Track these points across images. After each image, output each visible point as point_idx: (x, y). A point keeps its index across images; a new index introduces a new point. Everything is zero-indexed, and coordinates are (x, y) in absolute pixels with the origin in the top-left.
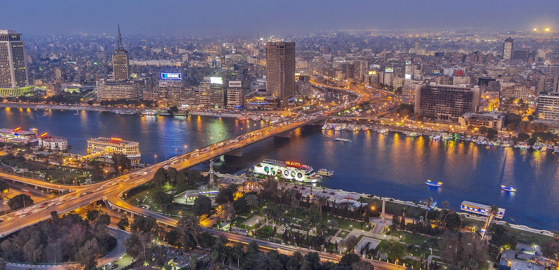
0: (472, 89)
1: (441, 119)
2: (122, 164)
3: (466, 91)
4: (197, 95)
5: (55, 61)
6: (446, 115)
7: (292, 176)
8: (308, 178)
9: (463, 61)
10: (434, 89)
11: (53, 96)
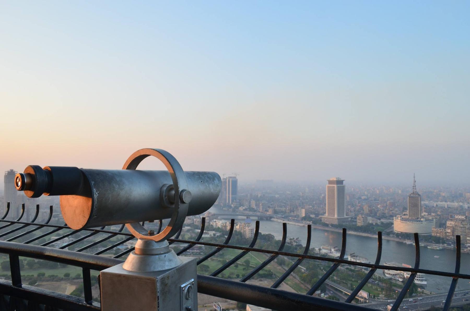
5: (365, 199)
11: (362, 226)
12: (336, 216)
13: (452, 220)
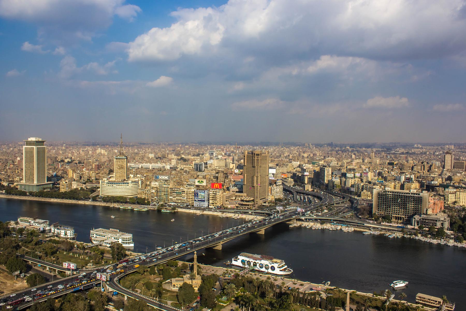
0: (421, 194)
1: (396, 219)
2: (118, 252)
3: (417, 196)
4: (183, 194)
6: (400, 216)
7: (266, 268)
8: (280, 271)
9: (412, 169)
10: (389, 193)
11: (66, 192)
12: (35, 182)
13: (156, 181)
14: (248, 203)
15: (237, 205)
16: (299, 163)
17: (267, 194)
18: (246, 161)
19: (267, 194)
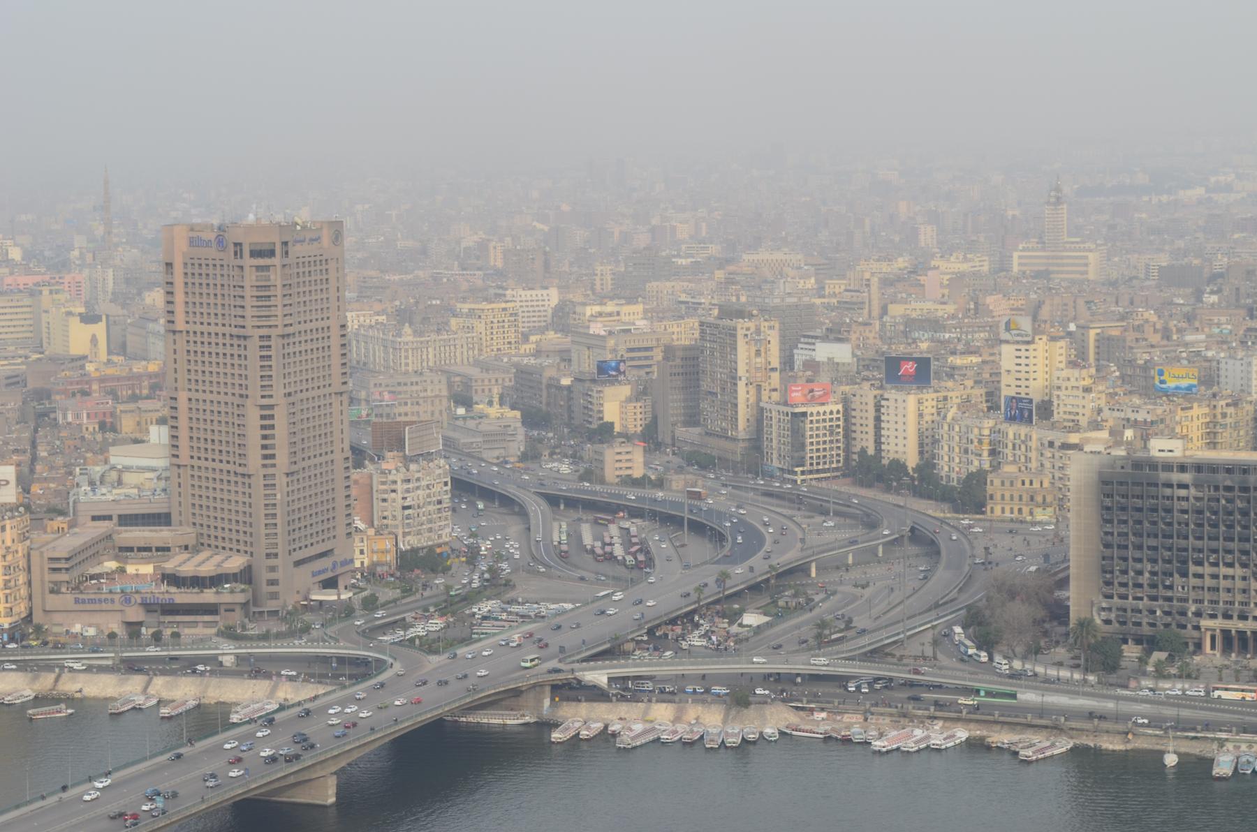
10: (1176, 477)
14: (209, 596)
15: (135, 614)
16: (553, 297)
17: (341, 521)
18: (179, 298)
19: (341, 521)
